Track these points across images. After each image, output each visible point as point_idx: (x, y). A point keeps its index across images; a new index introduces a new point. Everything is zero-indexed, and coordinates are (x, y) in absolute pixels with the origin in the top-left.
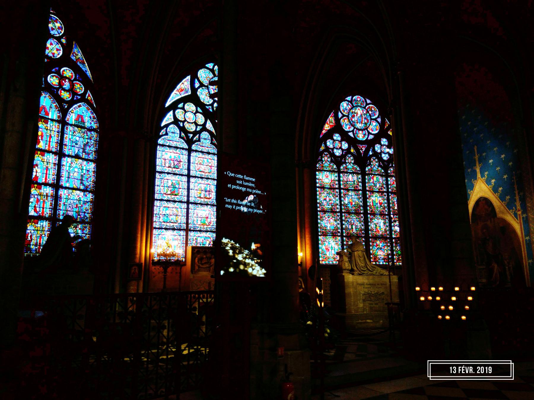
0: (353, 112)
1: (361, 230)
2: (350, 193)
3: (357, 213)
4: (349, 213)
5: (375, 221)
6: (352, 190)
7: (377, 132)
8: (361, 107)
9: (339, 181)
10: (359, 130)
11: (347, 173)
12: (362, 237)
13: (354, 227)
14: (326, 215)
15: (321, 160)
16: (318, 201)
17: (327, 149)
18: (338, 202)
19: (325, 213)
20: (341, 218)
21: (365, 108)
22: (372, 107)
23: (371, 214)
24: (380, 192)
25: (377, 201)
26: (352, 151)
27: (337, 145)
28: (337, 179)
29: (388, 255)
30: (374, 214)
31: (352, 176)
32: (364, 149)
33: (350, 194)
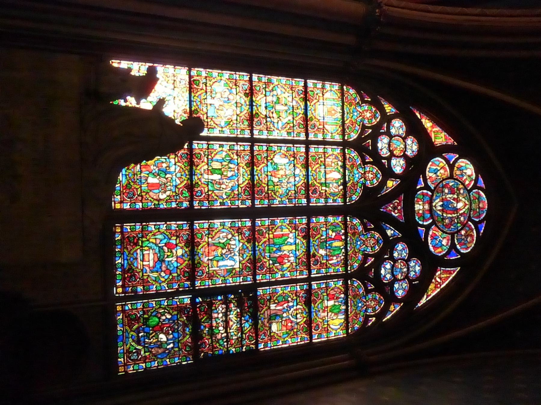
0: (459, 189)
1: (208, 198)
2: (300, 172)
3: (252, 188)
4: (252, 164)
5: (236, 244)
6: (307, 176)
7: (431, 248)
8: (470, 209)
9: (324, 143)
10: (430, 203)
11: (344, 167)
12: (191, 201)
13: (216, 177)
14: (244, 100)
15: (363, 101)
16: (274, 79)
17: (387, 119)
18: (275, 135)
19: (246, 95)
20: (237, 140)
21: (470, 219)
22: (472, 236)
23: (253, 229)
24: (309, 258)
25: (286, 249)
26: (391, 184)
27: (397, 145)
28: (328, 138)
29: (145, 282)
30: (253, 237)
31: (337, 180)
32: (395, 214)
33: (297, 172)
